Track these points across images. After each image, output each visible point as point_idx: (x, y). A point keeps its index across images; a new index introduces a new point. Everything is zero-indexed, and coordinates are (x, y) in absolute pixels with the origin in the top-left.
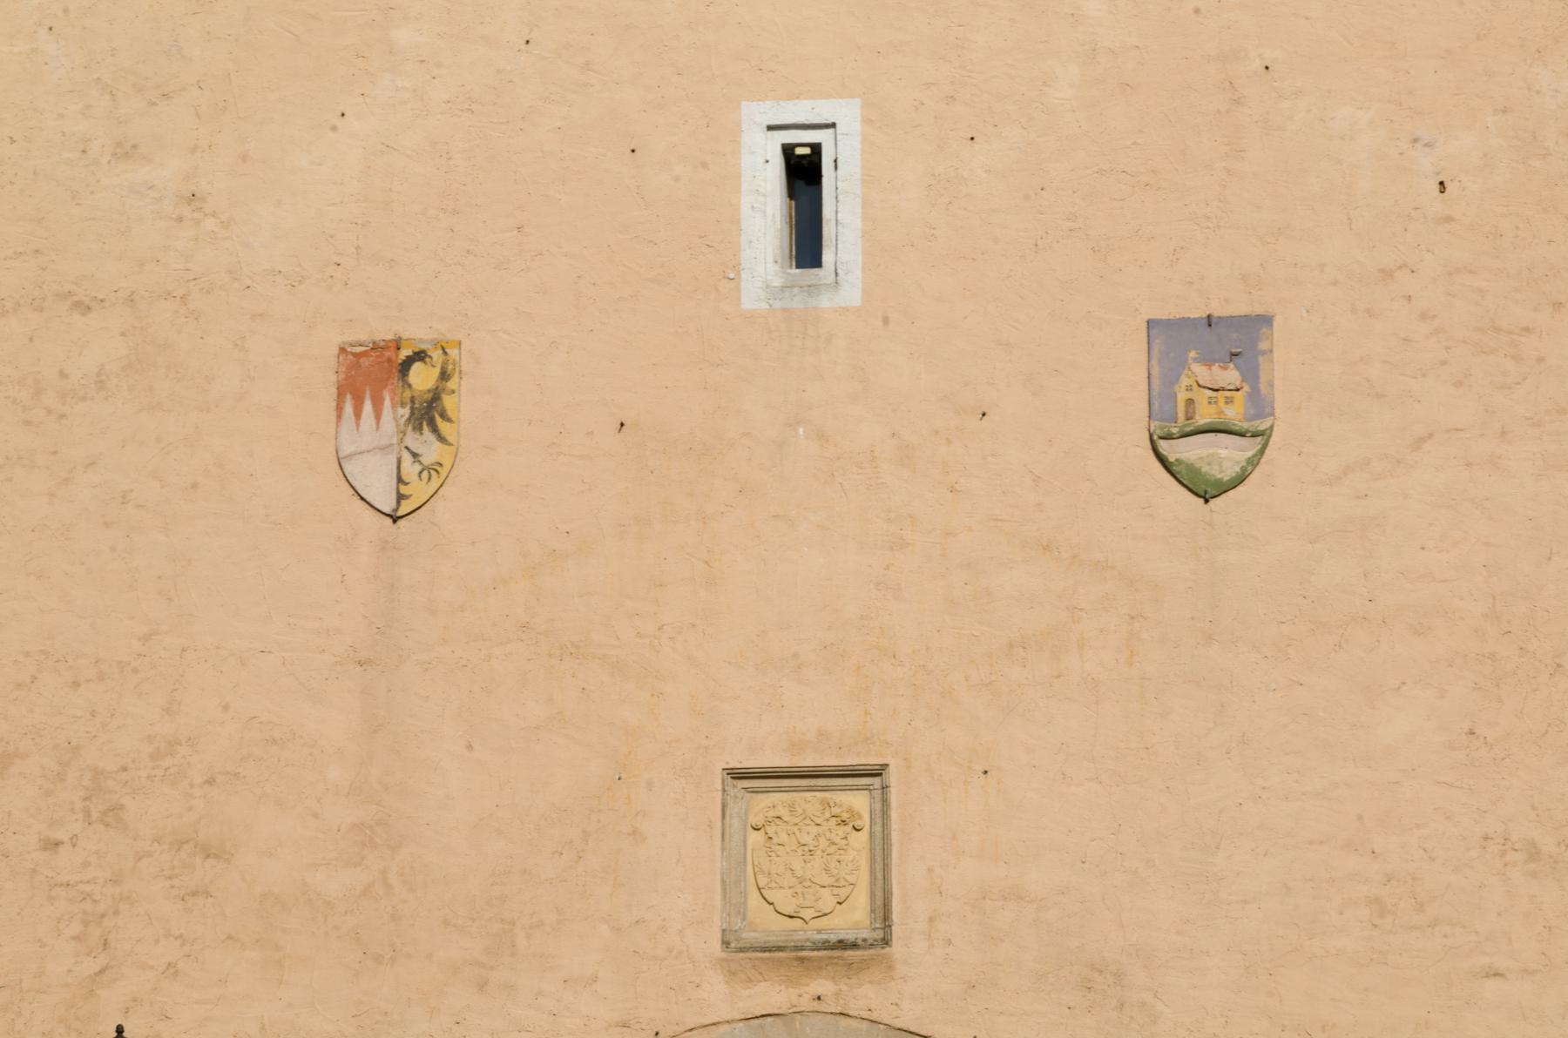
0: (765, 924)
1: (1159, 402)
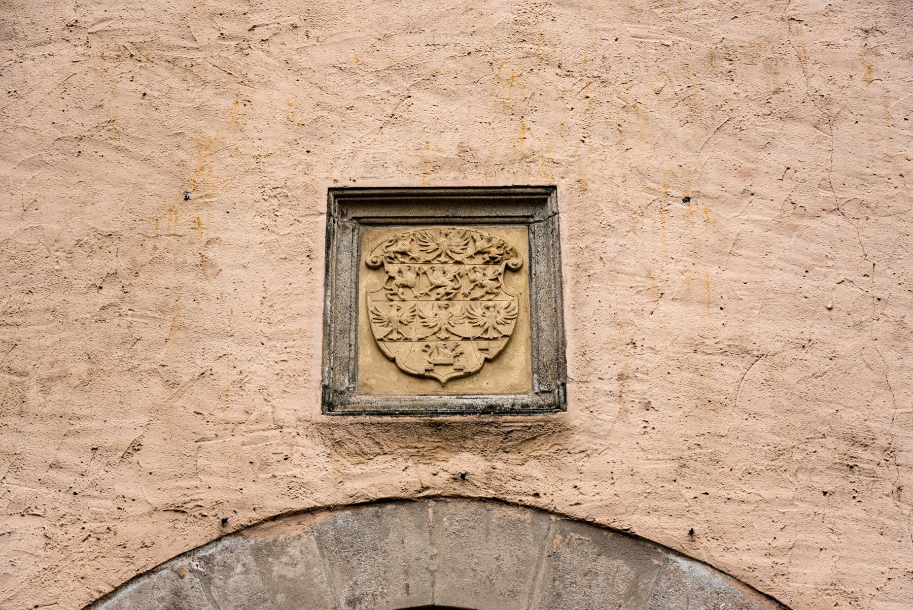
0: (383, 386)
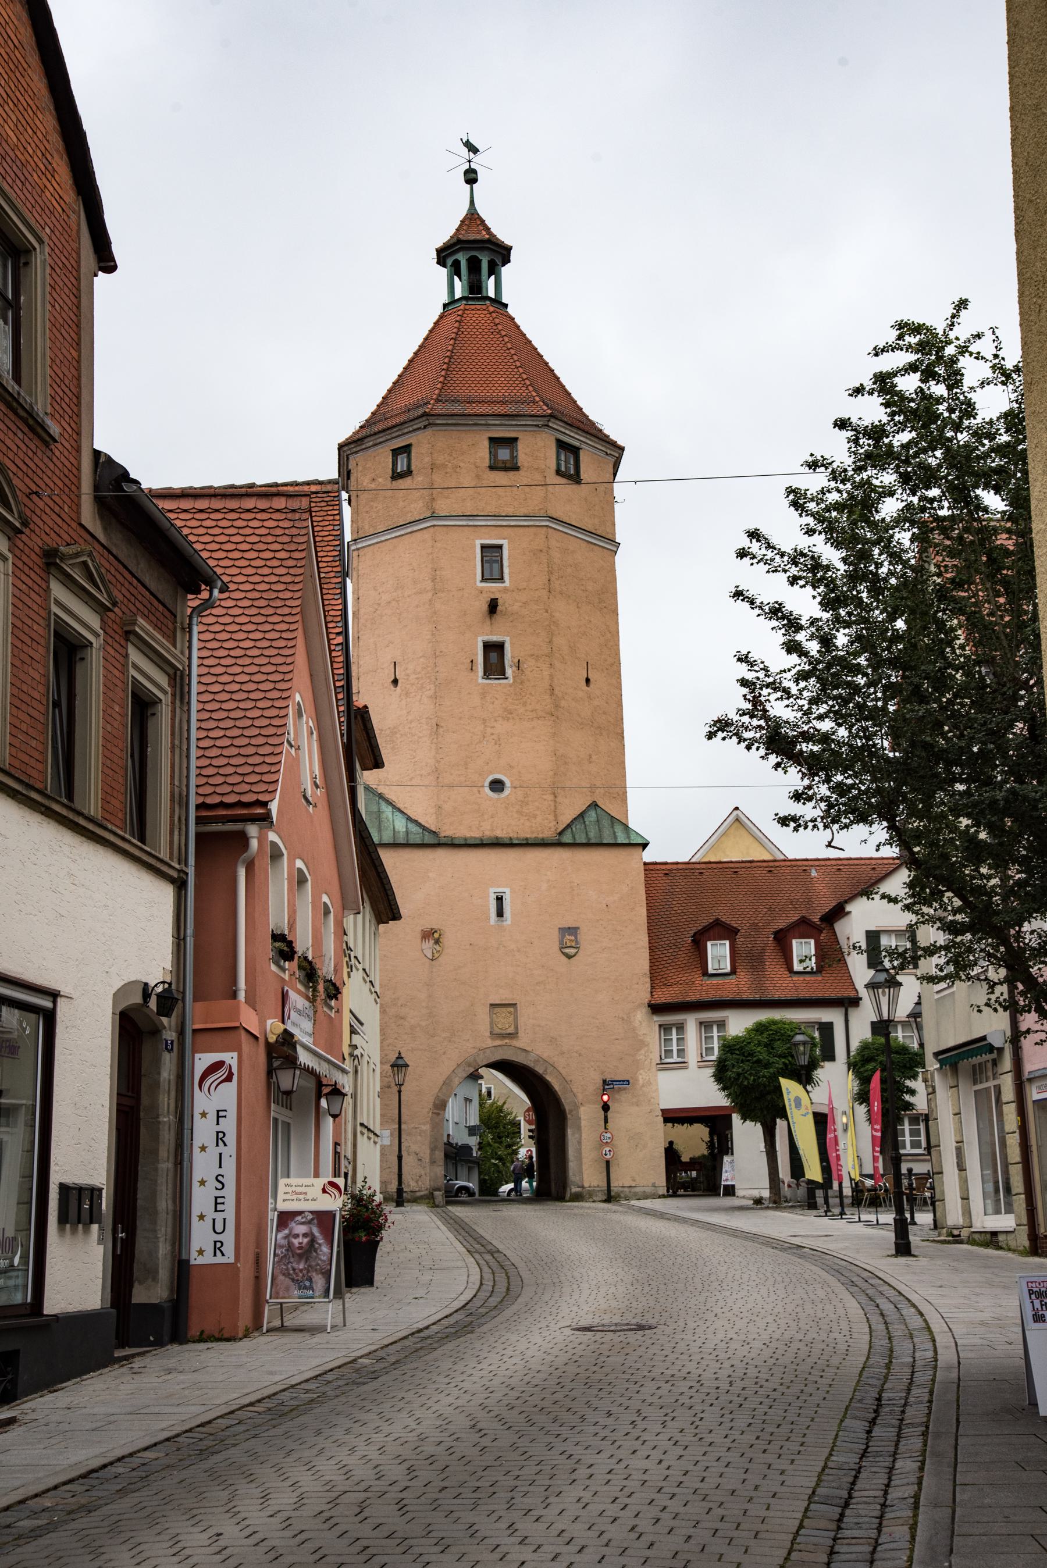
0: (497, 1031)
1: (561, 942)
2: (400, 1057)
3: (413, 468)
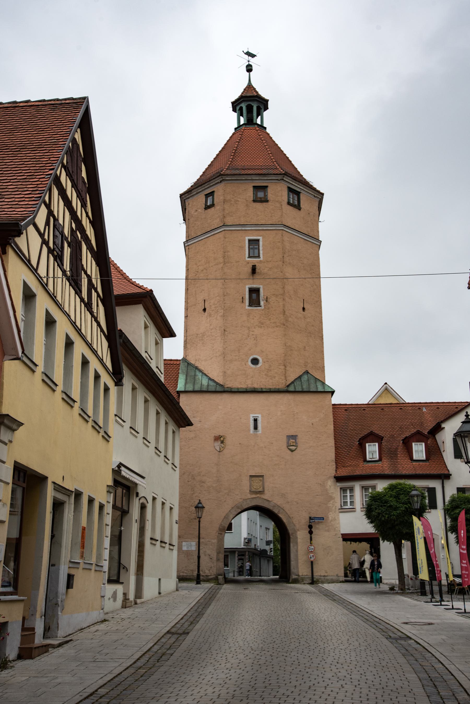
0: (253, 490)
1: (288, 443)
2: (200, 503)
3: (215, 203)
